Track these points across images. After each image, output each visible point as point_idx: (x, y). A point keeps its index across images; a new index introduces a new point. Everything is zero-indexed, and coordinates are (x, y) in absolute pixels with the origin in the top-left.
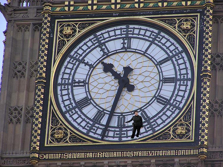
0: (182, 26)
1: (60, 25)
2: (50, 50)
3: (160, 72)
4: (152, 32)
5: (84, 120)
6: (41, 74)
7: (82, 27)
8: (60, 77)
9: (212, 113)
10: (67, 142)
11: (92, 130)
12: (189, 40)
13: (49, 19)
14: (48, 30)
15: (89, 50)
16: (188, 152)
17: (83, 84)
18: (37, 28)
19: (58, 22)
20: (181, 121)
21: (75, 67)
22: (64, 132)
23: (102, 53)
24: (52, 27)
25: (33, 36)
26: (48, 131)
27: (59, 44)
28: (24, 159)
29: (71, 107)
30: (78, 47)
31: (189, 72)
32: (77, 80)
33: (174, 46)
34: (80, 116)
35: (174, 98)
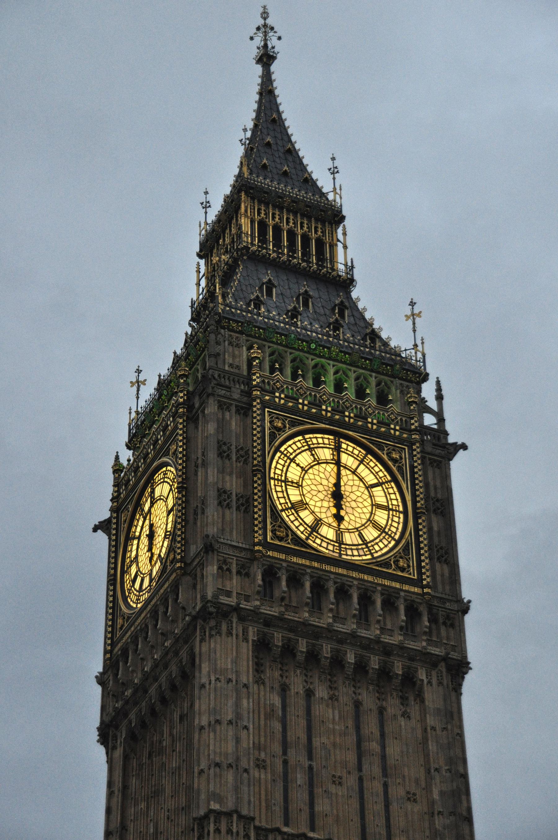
1: (269, 415)
7: (293, 424)
8: (272, 471)
12: (398, 471)
19: (268, 411)
21: (287, 464)
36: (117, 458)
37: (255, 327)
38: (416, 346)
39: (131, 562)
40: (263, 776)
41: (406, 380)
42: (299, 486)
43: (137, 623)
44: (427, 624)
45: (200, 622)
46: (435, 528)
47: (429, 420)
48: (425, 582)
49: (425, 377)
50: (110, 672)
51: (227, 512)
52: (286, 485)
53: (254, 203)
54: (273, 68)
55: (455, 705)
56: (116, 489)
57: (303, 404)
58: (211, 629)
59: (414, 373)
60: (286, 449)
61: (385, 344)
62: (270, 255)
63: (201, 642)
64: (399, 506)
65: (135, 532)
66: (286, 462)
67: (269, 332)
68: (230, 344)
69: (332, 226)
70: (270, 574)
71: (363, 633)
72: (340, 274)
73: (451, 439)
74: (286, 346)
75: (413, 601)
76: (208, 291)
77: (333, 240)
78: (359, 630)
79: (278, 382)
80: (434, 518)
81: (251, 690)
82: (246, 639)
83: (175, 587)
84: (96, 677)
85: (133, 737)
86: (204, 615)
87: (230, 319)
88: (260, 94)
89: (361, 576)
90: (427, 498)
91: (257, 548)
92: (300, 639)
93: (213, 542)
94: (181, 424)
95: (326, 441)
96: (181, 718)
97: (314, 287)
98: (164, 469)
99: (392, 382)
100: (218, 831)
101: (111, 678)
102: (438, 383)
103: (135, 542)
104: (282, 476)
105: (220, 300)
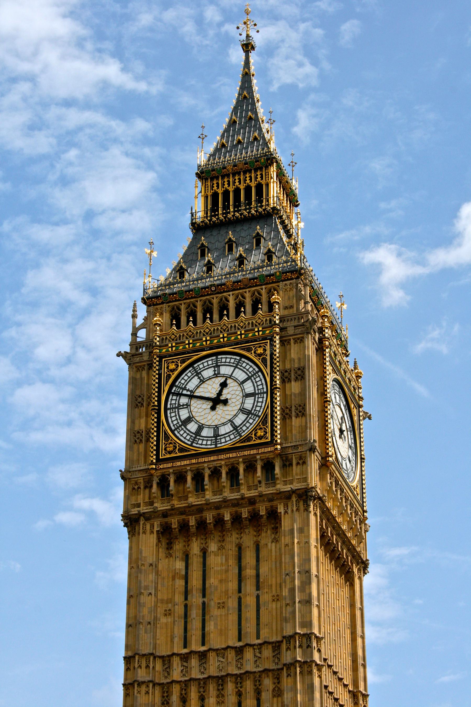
0: (257, 352)
2: (159, 383)
3: (243, 390)
4: (235, 359)
5: (188, 434)
6: (154, 403)
7: (183, 362)
8: (169, 403)
9: (284, 417)
10: (176, 453)
11: (195, 442)
12: (262, 362)
13: (158, 359)
14: (157, 368)
15: (189, 379)
16: (266, 450)
17: (186, 406)
19: (165, 361)
20: (260, 426)
22: (174, 446)
23: (199, 380)
24: (160, 365)
25: (148, 374)
26: (162, 446)
27: (166, 377)
28: (146, 471)
29: (178, 425)
30: (181, 378)
31: (265, 387)
32: (182, 404)
33: (253, 368)
34: (185, 432)
35: (254, 409)
41: (288, 279)
59: (292, 272)
67: (180, 293)
82: (152, 532)
92: (190, 517)
99: (278, 286)
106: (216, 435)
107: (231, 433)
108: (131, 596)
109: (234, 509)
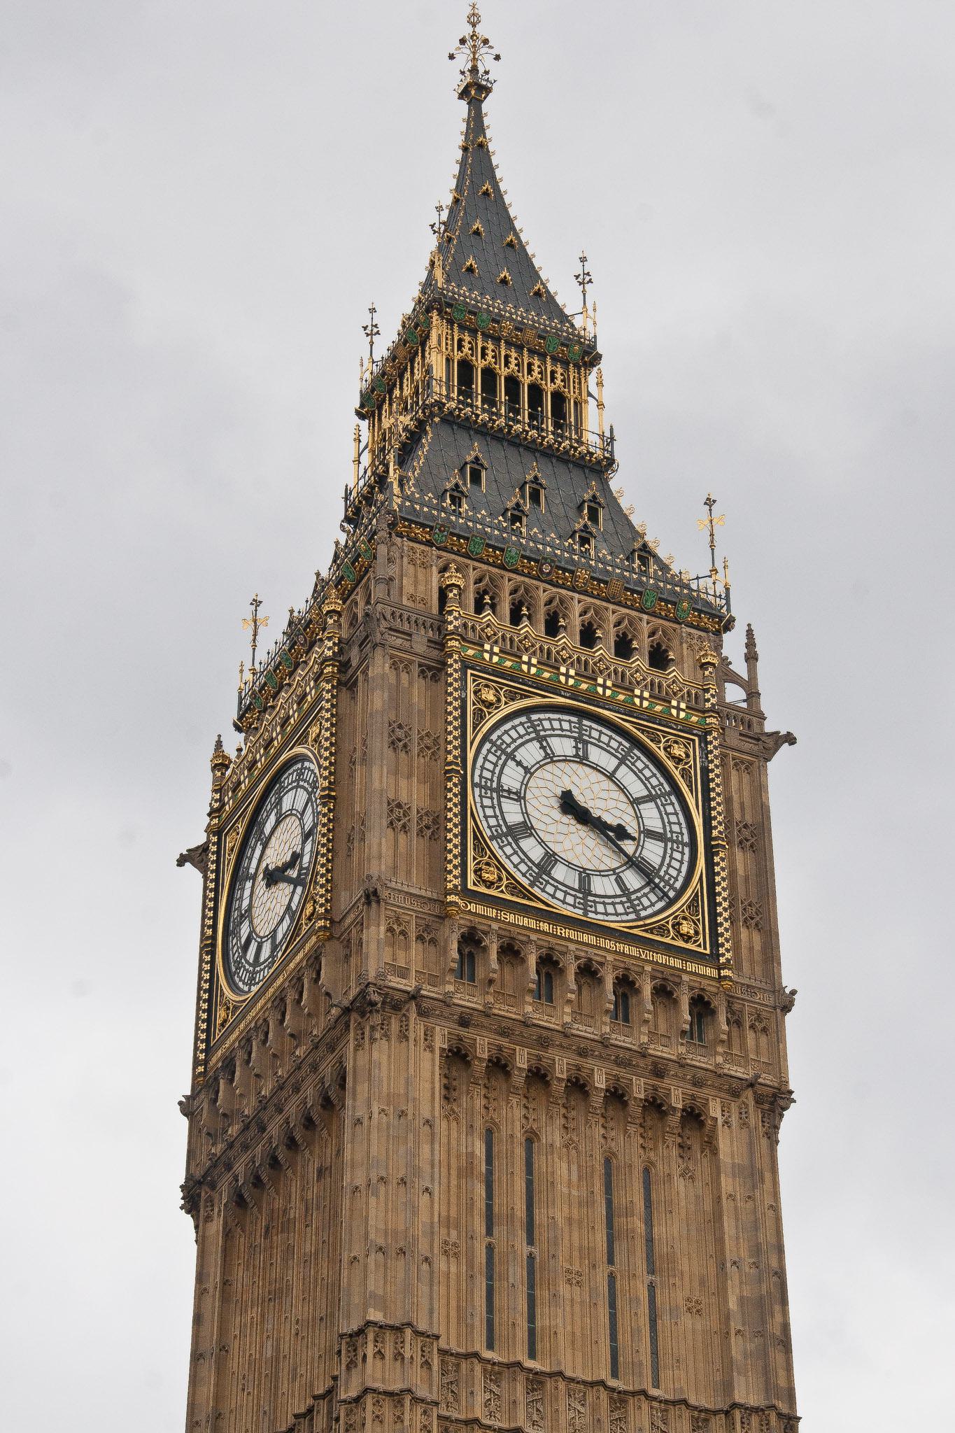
8: (477, 772)
18: (422, 672)
21: (501, 762)
24: (463, 679)
36: (219, 744)
37: (453, 534)
38: (715, 571)
39: (242, 916)
40: (453, 1269)
42: (519, 797)
43: (249, 1018)
44: (725, 1027)
45: (354, 1016)
46: (741, 872)
47: (734, 694)
48: (722, 960)
49: (728, 625)
50: (202, 1096)
51: (402, 837)
52: (499, 797)
53: (452, 329)
54: (485, 107)
55: (767, 1160)
56: (218, 796)
57: (530, 666)
58: (373, 1028)
59: (713, 616)
60: (499, 737)
61: (665, 568)
62: (477, 416)
63: (356, 1050)
64: (682, 834)
65: (248, 868)
66: (499, 758)
68: (412, 562)
69: (579, 369)
70: (471, 940)
71: (619, 1039)
72: (592, 450)
73: (769, 727)
74: (502, 567)
75: (703, 990)
76: (374, 473)
77: (580, 394)
78: (614, 1036)
79: (488, 626)
80: (739, 855)
81: (437, 1130)
82: (430, 1048)
83: (315, 961)
84: (180, 1103)
85: (240, 1201)
86: (361, 1006)
87: (411, 521)
88: (465, 149)
89: (620, 947)
90: (728, 823)
91: (450, 898)
93: (379, 888)
94: (328, 692)
95: (566, 726)
96: (321, 1172)
97: (549, 470)
98: (299, 766)
100: (380, 1354)
101: (205, 1105)
102: (750, 633)
103: (249, 884)
104: (492, 781)
105: (396, 489)
106: (585, 889)
107: (618, 900)
108: (382, 1178)
109: (616, 1071)
